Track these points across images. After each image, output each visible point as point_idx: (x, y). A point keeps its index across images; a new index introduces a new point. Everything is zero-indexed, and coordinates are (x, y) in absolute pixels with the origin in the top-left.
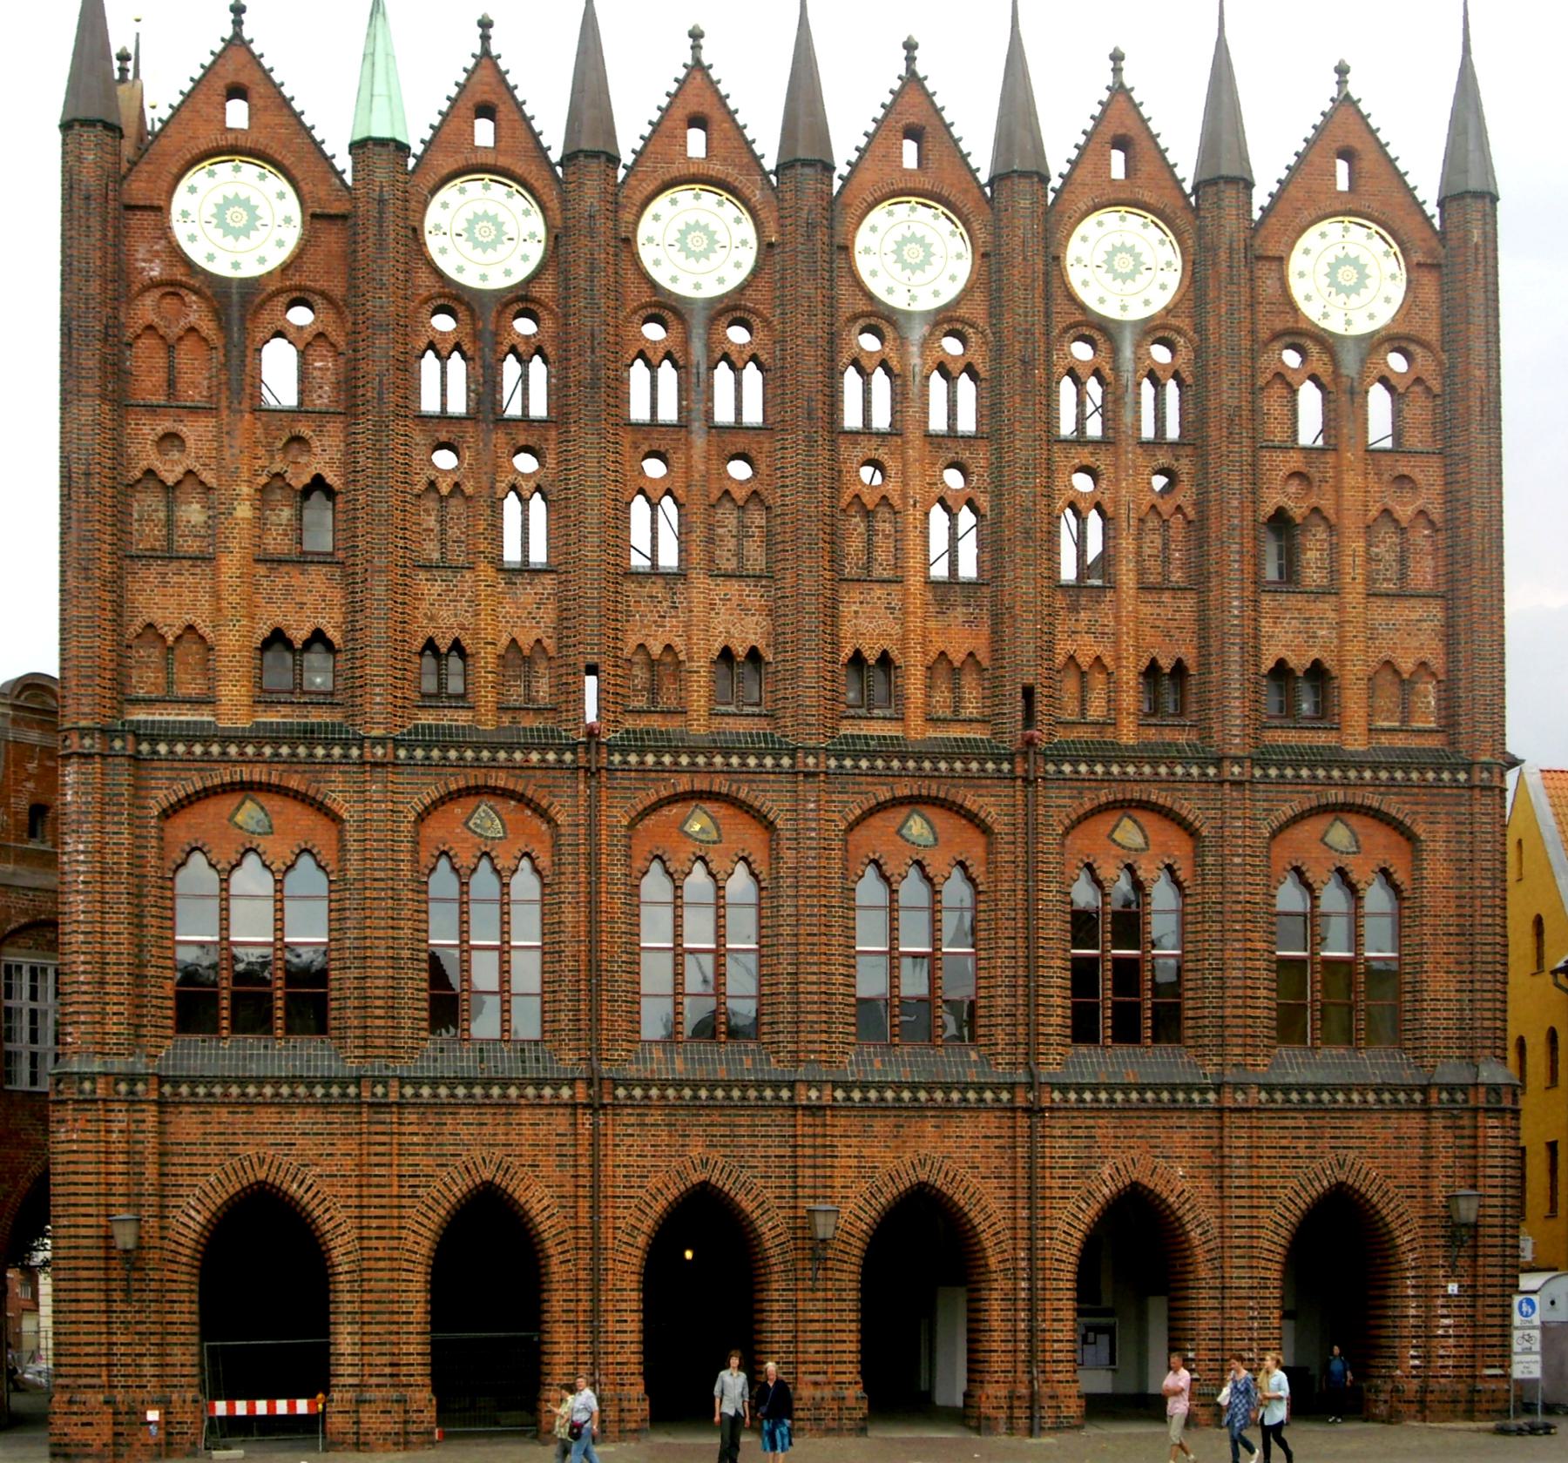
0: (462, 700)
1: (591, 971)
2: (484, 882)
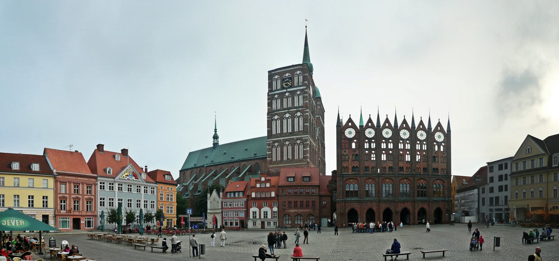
0: (368, 171)
1: (379, 191)
2: (370, 185)
